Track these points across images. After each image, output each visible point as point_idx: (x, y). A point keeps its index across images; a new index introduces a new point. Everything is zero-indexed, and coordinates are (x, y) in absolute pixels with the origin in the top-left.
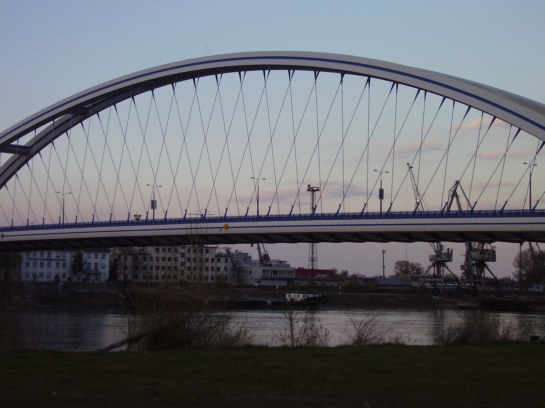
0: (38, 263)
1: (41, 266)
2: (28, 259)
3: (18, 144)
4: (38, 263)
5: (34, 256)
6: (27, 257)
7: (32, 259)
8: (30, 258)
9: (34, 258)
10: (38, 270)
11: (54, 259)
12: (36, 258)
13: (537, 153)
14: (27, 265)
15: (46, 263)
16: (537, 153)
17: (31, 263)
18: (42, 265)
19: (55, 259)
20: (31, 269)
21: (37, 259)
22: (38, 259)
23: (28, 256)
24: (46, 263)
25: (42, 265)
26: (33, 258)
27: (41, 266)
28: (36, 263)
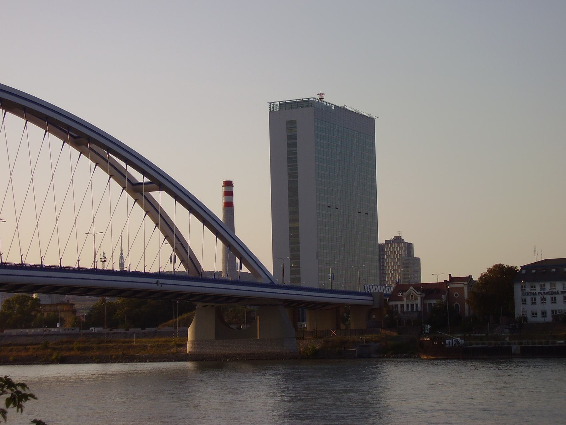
0: (538, 298)
1: (533, 303)
2: (523, 294)
3: (145, 181)
4: (538, 298)
5: (532, 290)
6: (522, 292)
7: (529, 294)
8: (525, 293)
9: (532, 293)
10: (539, 307)
11: (560, 293)
12: (535, 292)
13: (4, 118)
14: (524, 302)
15: (548, 298)
16: (4, 118)
17: (529, 298)
18: (543, 300)
19: (561, 292)
20: (529, 308)
21: (535, 293)
22: (538, 294)
23: (524, 290)
24: (548, 298)
25: (543, 300)
26: (530, 293)
27: (533, 303)
28: (535, 298)
